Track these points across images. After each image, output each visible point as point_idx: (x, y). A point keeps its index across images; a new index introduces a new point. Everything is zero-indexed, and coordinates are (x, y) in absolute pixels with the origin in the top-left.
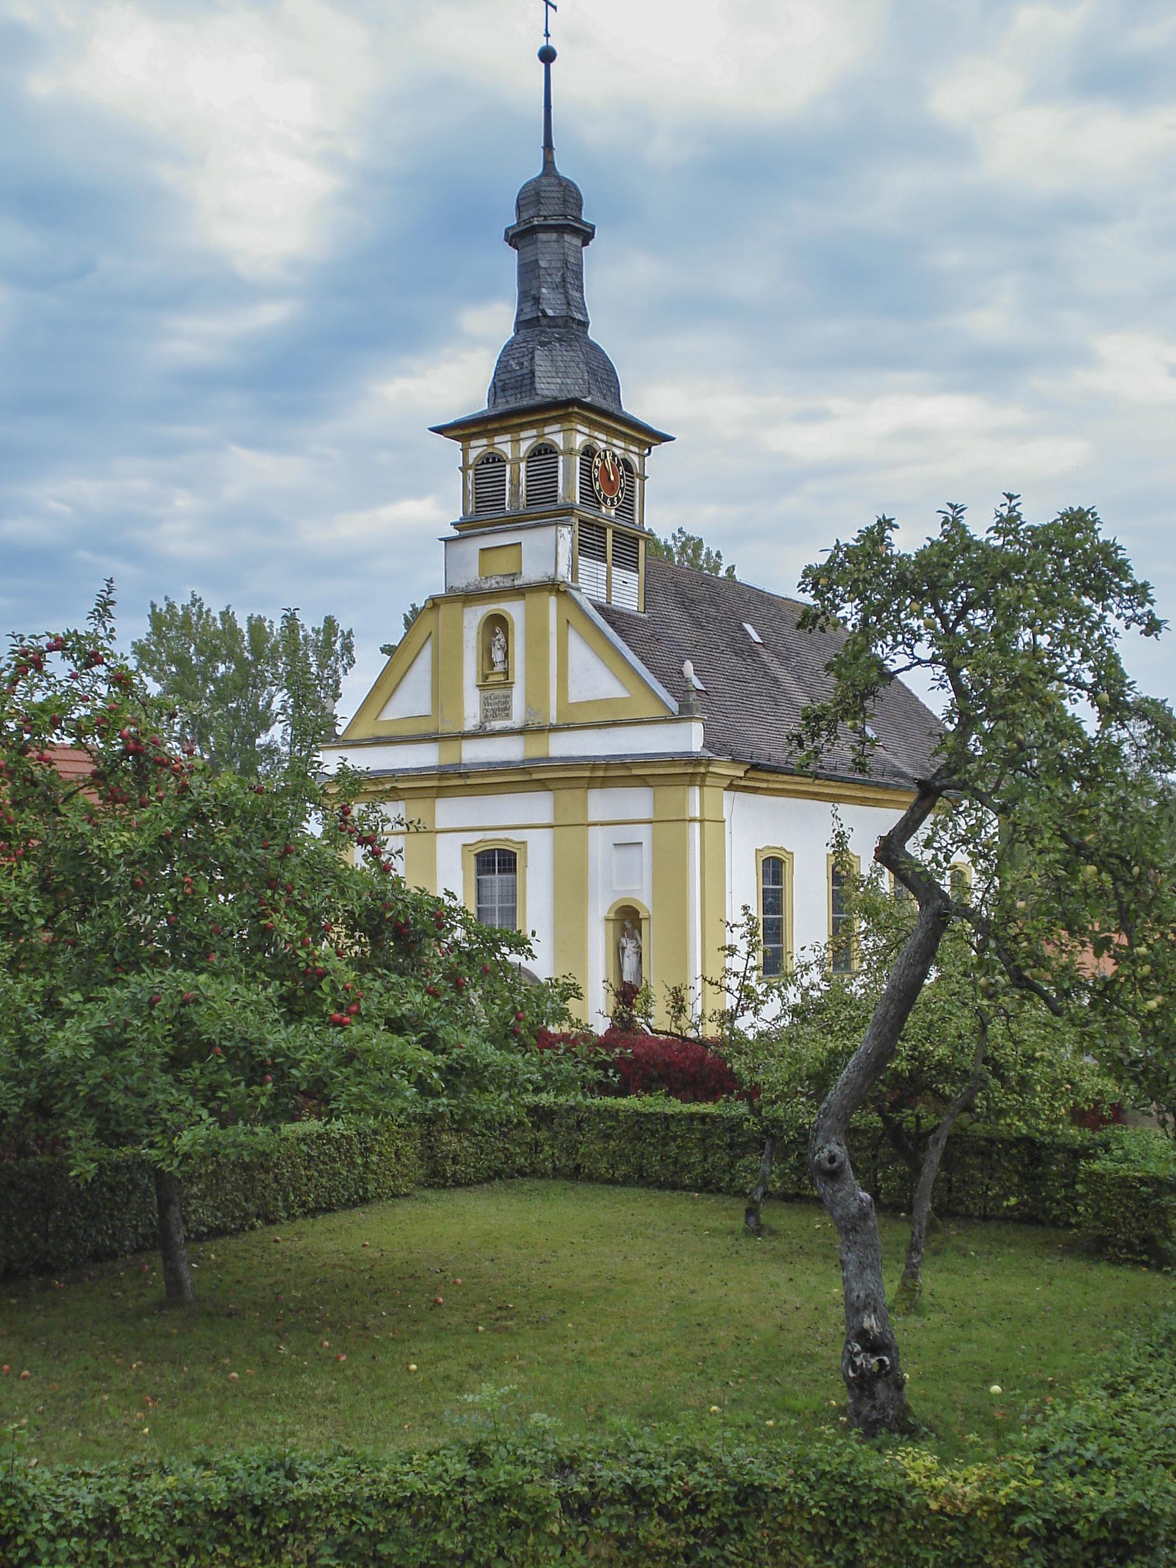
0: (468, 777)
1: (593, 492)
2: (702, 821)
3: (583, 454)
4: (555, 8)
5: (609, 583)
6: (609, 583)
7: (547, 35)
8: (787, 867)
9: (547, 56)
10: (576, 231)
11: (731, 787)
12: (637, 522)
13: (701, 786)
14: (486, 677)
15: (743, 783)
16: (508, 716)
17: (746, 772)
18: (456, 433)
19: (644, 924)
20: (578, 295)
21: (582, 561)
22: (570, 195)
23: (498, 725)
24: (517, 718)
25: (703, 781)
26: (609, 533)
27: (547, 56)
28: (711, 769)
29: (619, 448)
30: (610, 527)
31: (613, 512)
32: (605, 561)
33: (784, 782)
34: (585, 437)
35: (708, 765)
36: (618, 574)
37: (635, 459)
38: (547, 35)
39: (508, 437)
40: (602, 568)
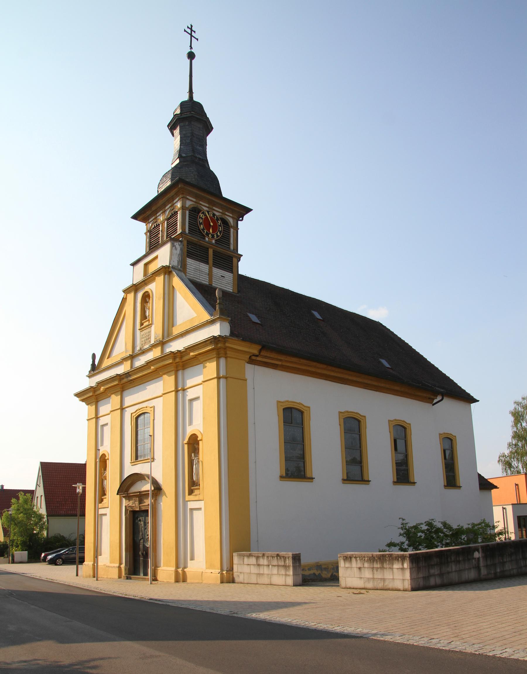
0: (130, 376)
1: (199, 230)
2: (226, 378)
3: (192, 211)
4: (197, 39)
5: (210, 274)
6: (210, 274)
7: (191, 48)
8: (305, 414)
9: (191, 56)
10: (198, 120)
11: (252, 361)
12: (232, 247)
13: (226, 358)
14: (142, 324)
15: (259, 359)
16: (150, 342)
17: (260, 351)
18: (141, 217)
19: (200, 442)
20: (200, 148)
21: (189, 261)
22: (199, 107)
23: (147, 346)
24: (152, 342)
25: (226, 354)
26: (211, 252)
27: (191, 56)
28: (227, 345)
29: (218, 212)
30: (211, 248)
31: (214, 241)
32: (207, 262)
33: (292, 362)
34: (193, 203)
35: (225, 342)
36: (217, 272)
37: (231, 221)
38: (191, 48)
39: (161, 212)
40: (205, 267)
